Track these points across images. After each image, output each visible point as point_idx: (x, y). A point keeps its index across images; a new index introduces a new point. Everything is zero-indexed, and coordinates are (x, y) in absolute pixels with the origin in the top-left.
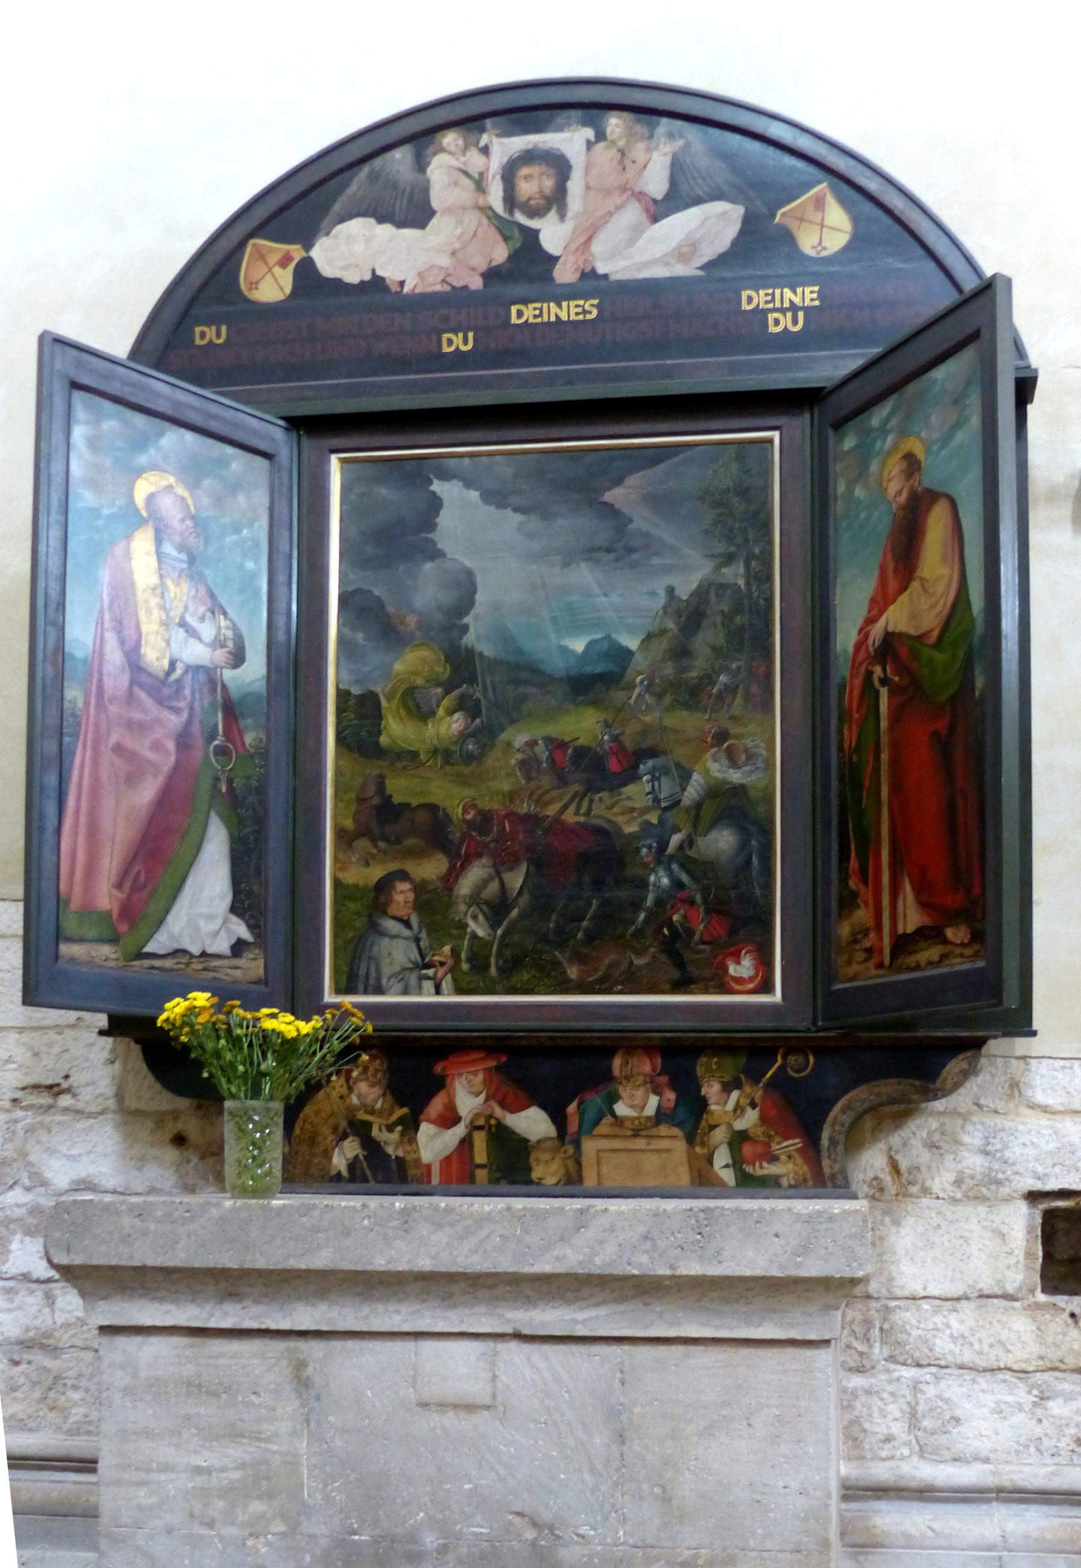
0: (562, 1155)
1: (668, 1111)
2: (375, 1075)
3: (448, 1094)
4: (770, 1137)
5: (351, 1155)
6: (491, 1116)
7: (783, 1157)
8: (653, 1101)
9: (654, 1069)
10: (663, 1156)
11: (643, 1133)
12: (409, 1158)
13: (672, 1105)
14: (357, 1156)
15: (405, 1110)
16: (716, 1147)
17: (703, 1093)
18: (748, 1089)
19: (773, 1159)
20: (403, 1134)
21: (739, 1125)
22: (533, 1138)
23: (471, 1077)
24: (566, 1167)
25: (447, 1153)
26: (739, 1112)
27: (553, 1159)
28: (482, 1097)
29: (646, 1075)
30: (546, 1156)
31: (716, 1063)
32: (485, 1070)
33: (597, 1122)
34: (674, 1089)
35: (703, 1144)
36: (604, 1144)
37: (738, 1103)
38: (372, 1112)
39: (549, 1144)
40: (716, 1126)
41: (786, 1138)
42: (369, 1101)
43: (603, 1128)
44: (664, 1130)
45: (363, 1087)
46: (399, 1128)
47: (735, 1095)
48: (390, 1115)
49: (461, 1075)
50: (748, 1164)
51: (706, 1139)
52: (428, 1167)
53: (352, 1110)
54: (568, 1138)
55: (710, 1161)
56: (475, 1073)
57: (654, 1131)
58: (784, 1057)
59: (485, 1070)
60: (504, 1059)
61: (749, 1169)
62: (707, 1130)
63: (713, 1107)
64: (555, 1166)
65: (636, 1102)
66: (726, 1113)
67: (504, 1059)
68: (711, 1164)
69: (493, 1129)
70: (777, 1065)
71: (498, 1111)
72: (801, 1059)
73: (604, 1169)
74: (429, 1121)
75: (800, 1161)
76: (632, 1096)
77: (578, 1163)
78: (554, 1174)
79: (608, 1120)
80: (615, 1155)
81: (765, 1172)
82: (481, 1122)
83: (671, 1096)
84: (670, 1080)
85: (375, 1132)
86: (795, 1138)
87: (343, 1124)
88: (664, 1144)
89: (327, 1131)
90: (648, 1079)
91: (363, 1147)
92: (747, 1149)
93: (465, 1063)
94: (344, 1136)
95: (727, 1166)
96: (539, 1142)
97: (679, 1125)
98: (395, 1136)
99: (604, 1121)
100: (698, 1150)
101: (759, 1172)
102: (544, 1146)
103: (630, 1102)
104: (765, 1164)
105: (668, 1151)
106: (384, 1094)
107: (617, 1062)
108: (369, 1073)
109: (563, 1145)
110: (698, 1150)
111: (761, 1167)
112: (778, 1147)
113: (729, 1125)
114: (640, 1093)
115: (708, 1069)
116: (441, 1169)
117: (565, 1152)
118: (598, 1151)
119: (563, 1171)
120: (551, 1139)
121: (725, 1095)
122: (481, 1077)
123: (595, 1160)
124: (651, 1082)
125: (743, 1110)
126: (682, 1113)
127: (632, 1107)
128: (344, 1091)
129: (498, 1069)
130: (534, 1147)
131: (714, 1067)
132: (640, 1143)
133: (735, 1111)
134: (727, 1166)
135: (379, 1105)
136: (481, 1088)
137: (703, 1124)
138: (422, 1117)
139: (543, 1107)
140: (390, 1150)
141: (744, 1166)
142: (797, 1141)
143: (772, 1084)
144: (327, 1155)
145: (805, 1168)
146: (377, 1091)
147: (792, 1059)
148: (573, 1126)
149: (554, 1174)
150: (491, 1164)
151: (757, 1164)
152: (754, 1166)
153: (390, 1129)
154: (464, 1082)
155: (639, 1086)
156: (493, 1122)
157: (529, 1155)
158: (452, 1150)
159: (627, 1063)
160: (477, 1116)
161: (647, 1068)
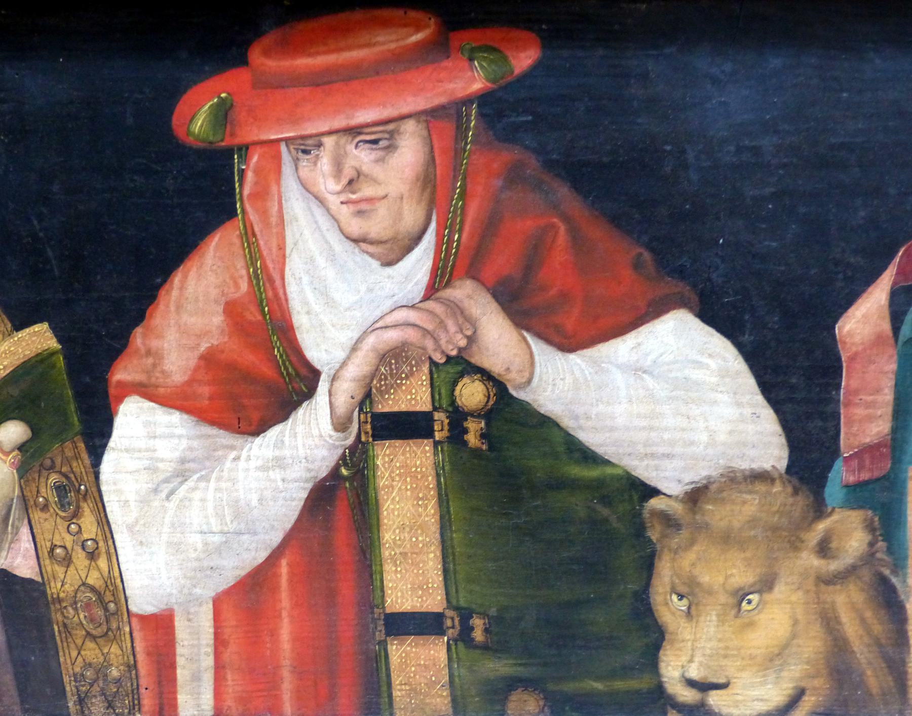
0: (809, 560)
3: (253, 255)
27: (766, 584)
32: (430, 116)
59: (430, 116)
69: (474, 430)
74: (148, 392)
109: (819, 509)
116: (219, 642)
117: (824, 549)
120: (760, 477)
130: (668, 521)
136: (412, 216)
138: (122, 373)
150: (465, 615)
154: (329, 186)
157: (648, 565)
158: (276, 538)
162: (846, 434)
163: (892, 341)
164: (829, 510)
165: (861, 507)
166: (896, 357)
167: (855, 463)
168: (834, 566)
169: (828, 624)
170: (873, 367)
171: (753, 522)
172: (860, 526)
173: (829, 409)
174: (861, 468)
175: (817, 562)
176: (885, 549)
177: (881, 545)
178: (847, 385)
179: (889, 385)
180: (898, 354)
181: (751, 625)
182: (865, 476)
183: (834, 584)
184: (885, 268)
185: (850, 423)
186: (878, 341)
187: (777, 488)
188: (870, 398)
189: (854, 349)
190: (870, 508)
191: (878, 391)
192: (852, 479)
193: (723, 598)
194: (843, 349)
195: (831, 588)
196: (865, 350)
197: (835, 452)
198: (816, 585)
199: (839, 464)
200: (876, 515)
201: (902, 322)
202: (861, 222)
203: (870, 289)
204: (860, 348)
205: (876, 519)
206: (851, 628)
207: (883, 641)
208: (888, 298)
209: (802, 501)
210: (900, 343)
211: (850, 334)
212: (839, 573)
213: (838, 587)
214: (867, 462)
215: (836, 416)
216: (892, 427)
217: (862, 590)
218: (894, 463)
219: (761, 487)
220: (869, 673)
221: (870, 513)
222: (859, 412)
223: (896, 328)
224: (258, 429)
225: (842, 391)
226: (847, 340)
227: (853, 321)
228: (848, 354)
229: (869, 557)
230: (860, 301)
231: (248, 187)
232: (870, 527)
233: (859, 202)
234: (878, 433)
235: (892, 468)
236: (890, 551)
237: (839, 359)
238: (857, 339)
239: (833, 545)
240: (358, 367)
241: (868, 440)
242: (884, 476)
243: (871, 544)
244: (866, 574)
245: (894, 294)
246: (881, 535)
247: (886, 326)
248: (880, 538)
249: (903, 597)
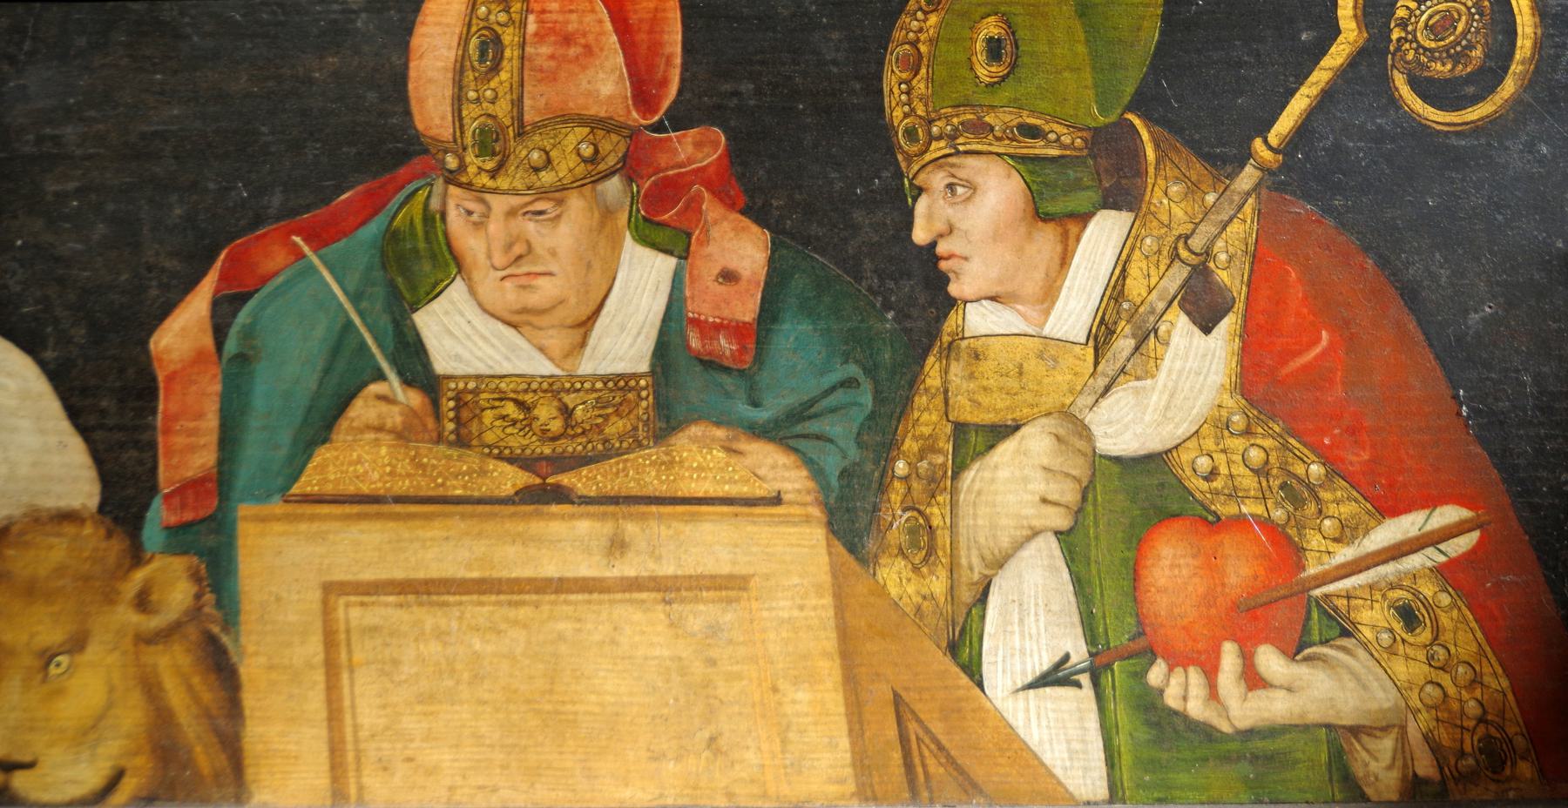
1: (725, 345)
9: (643, 92)
10: (700, 614)
11: (578, 481)
13: (746, 309)
16: (1000, 562)
17: (920, 235)
24: (151, 688)
26: (1123, 344)
27: (77, 644)
29: (599, 125)
31: (994, 49)
34: (757, 213)
37: (1116, 291)
40: (1001, 432)
41: (1388, 508)
50: (1178, 661)
51: (937, 516)
54: (158, 515)
62: (944, 458)
63: (980, 320)
65: (546, 290)
66: (1051, 348)
68: (973, 670)
70: (1337, 55)
73: (367, 712)
76: (520, 256)
80: (431, 619)
81: (1274, 707)
84: (740, 152)
86: (1430, 502)
90: (613, 149)
95: (1056, 676)
99: (362, 410)
100: (894, 575)
103: (509, 296)
104: (1270, 660)
105: (730, 586)
109: (137, 556)
110: (894, 575)
111: (1253, 679)
112: (1344, 554)
117: (143, 602)
118: (332, 590)
119: (132, 716)
120: (68, 517)
121: (1046, 240)
123: (314, 648)
124: (630, 168)
125: (1146, 335)
127: (518, 319)
131: (985, 71)
133: (1101, 336)
134: (1056, 676)
137: (926, 418)
141: (1156, 675)
142: (1448, 515)
151: (1230, 657)
152: (1211, 673)
155: (557, 193)
162: (166, 466)
163: (215, 358)
164: (149, 555)
165: (185, 553)
166: (220, 377)
167: (176, 501)
168: (154, 623)
169: (149, 691)
170: (194, 388)
171: (60, 571)
172: (185, 575)
173: (145, 437)
174: (183, 506)
175: (134, 618)
176: (214, 602)
177: (209, 597)
178: (165, 410)
179: (213, 408)
180: (223, 373)
181: (59, 692)
182: (188, 516)
183: (156, 644)
184: (204, 273)
185: (169, 453)
186: (199, 358)
187: (88, 530)
188: (192, 425)
189: (172, 368)
190: (195, 554)
191: (200, 416)
192: (173, 519)
193: (27, 660)
194: (160, 367)
195: (152, 649)
196: (184, 369)
197: (153, 489)
198: (136, 645)
199: (157, 503)
200: (203, 562)
201: (226, 335)
202: (178, 221)
203: (189, 298)
204: (179, 366)
205: (203, 566)
206: (176, 697)
207: (214, 712)
208: (210, 307)
209: (116, 547)
210: (224, 360)
211: (168, 350)
212: (162, 630)
213: (161, 647)
214: (191, 500)
215: (152, 446)
216: (219, 458)
217: (189, 651)
218: (221, 502)
219: (69, 529)
220: (198, 749)
221: (195, 560)
222: (179, 441)
223: (219, 344)
225: (160, 417)
226: (165, 356)
227: (170, 335)
228: (166, 373)
229: (195, 613)
230: (177, 312)
232: (195, 577)
233: (174, 198)
234: (203, 465)
235: (219, 509)
236: (219, 604)
237: (154, 379)
238: (175, 356)
239: (154, 597)
241: (190, 474)
242: (210, 516)
243: (198, 596)
244: (192, 632)
245: (216, 304)
246: (209, 585)
247: (208, 341)
248: (208, 589)
249: (235, 659)
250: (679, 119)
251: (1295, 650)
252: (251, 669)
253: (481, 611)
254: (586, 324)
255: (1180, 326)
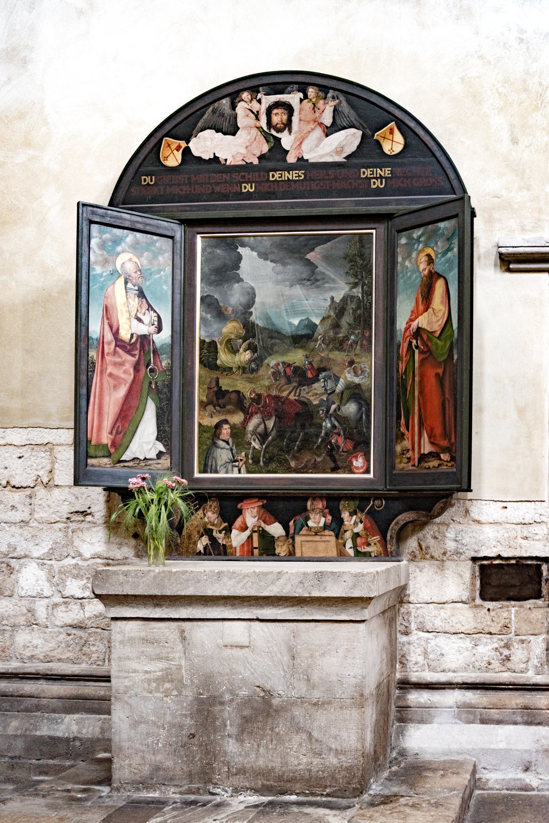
0: (287, 543)
2: (214, 509)
4: (367, 535)
5: (205, 544)
6: (260, 527)
7: (373, 544)
8: (323, 520)
9: (323, 507)
10: (326, 543)
11: (318, 534)
12: (228, 544)
13: (330, 522)
14: (207, 544)
15: (226, 524)
18: (359, 515)
19: (369, 545)
20: (225, 534)
21: (356, 530)
22: (276, 536)
23: (252, 510)
24: (289, 548)
25: (243, 542)
27: (284, 545)
28: (257, 518)
29: (320, 509)
30: (281, 544)
33: (301, 529)
34: (331, 515)
35: (342, 538)
36: (304, 538)
38: (213, 525)
39: (282, 539)
40: (347, 531)
41: (374, 536)
42: (212, 520)
43: (303, 532)
44: (327, 532)
45: (209, 514)
46: (224, 532)
47: (355, 517)
48: (220, 526)
49: (248, 509)
52: (235, 548)
53: (205, 524)
54: (290, 536)
55: (344, 546)
56: (254, 508)
57: (323, 533)
58: (373, 501)
60: (265, 502)
61: (359, 549)
63: (346, 523)
64: (285, 548)
65: (316, 521)
66: (351, 525)
67: (265, 502)
70: (371, 505)
71: (263, 525)
72: (380, 502)
73: (304, 549)
74: (235, 528)
75: (379, 545)
76: (315, 518)
77: (294, 546)
78: (284, 551)
79: (305, 528)
80: (308, 543)
81: (366, 550)
82: (256, 529)
83: (330, 518)
85: (214, 534)
87: (202, 530)
88: (327, 538)
89: (195, 533)
91: (210, 540)
92: (359, 540)
93: (250, 503)
94: (202, 536)
95: (351, 548)
96: (278, 537)
97: (332, 530)
98: (222, 535)
99: (304, 529)
100: (340, 541)
101: (363, 550)
102: (280, 539)
104: (365, 547)
105: (328, 541)
106: (218, 518)
107: (309, 503)
108: (212, 508)
110: (340, 541)
111: (364, 548)
113: (352, 531)
114: (318, 516)
115: (344, 507)
119: (287, 550)
122: (256, 509)
123: (300, 545)
124: (322, 512)
125: (357, 524)
126: (334, 526)
127: (315, 522)
128: (202, 515)
129: (263, 506)
132: (317, 538)
133: (354, 524)
134: (351, 548)
135: (216, 522)
137: (342, 530)
138: (233, 527)
139: (280, 523)
140: (220, 541)
142: (378, 537)
143: (369, 513)
144: (195, 543)
145: (381, 549)
146: (215, 516)
147: (376, 502)
148: (292, 531)
149: (284, 551)
153: (220, 532)
154: (250, 512)
156: (261, 529)
157: (274, 543)
159: (313, 504)
160: (254, 526)
161: (320, 506)
206: (291, 549)
224: (244, 532)
231: (243, 512)
240: (252, 527)
250: (326, 508)
251: (367, 546)
252: (296, 547)
253: (311, 543)
254: (319, 523)
255: (359, 523)
